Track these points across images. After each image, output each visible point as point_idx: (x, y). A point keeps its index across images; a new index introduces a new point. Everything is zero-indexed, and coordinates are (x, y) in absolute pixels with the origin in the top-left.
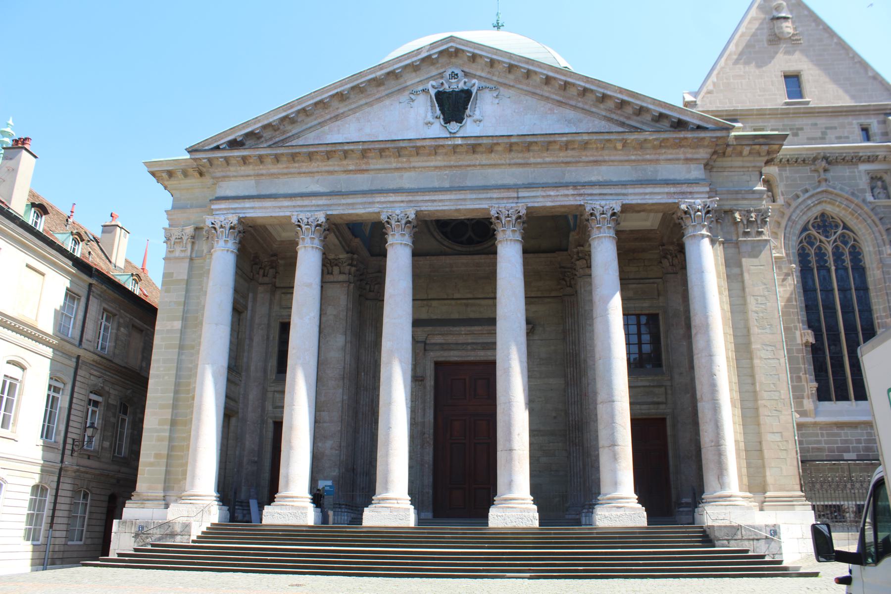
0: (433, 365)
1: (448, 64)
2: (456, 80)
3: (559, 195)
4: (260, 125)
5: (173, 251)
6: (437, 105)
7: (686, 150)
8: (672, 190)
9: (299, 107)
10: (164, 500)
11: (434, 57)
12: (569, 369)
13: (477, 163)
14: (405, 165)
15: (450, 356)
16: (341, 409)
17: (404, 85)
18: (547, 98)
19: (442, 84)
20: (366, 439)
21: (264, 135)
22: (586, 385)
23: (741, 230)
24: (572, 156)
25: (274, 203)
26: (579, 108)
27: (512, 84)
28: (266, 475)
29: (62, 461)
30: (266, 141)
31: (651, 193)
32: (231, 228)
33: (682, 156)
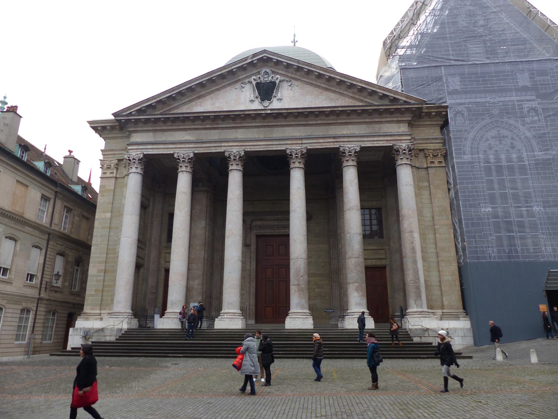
0: (255, 237)
1: (263, 66)
2: (267, 76)
3: (324, 142)
4: (155, 101)
5: (105, 173)
6: (256, 90)
7: (397, 115)
8: (389, 138)
9: (178, 91)
10: (100, 316)
11: (254, 62)
12: (331, 240)
13: (279, 124)
14: (239, 125)
16: (203, 262)
17: (238, 79)
18: (319, 87)
19: (260, 78)
21: (158, 107)
22: (341, 248)
23: (429, 162)
24: (333, 120)
25: (164, 146)
26: (337, 92)
27: (299, 78)
28: (160, 300)
29: (39, 294)
30: (159, 110)
31: (377, 141)
32: (139, 160)
33: (395, 119)
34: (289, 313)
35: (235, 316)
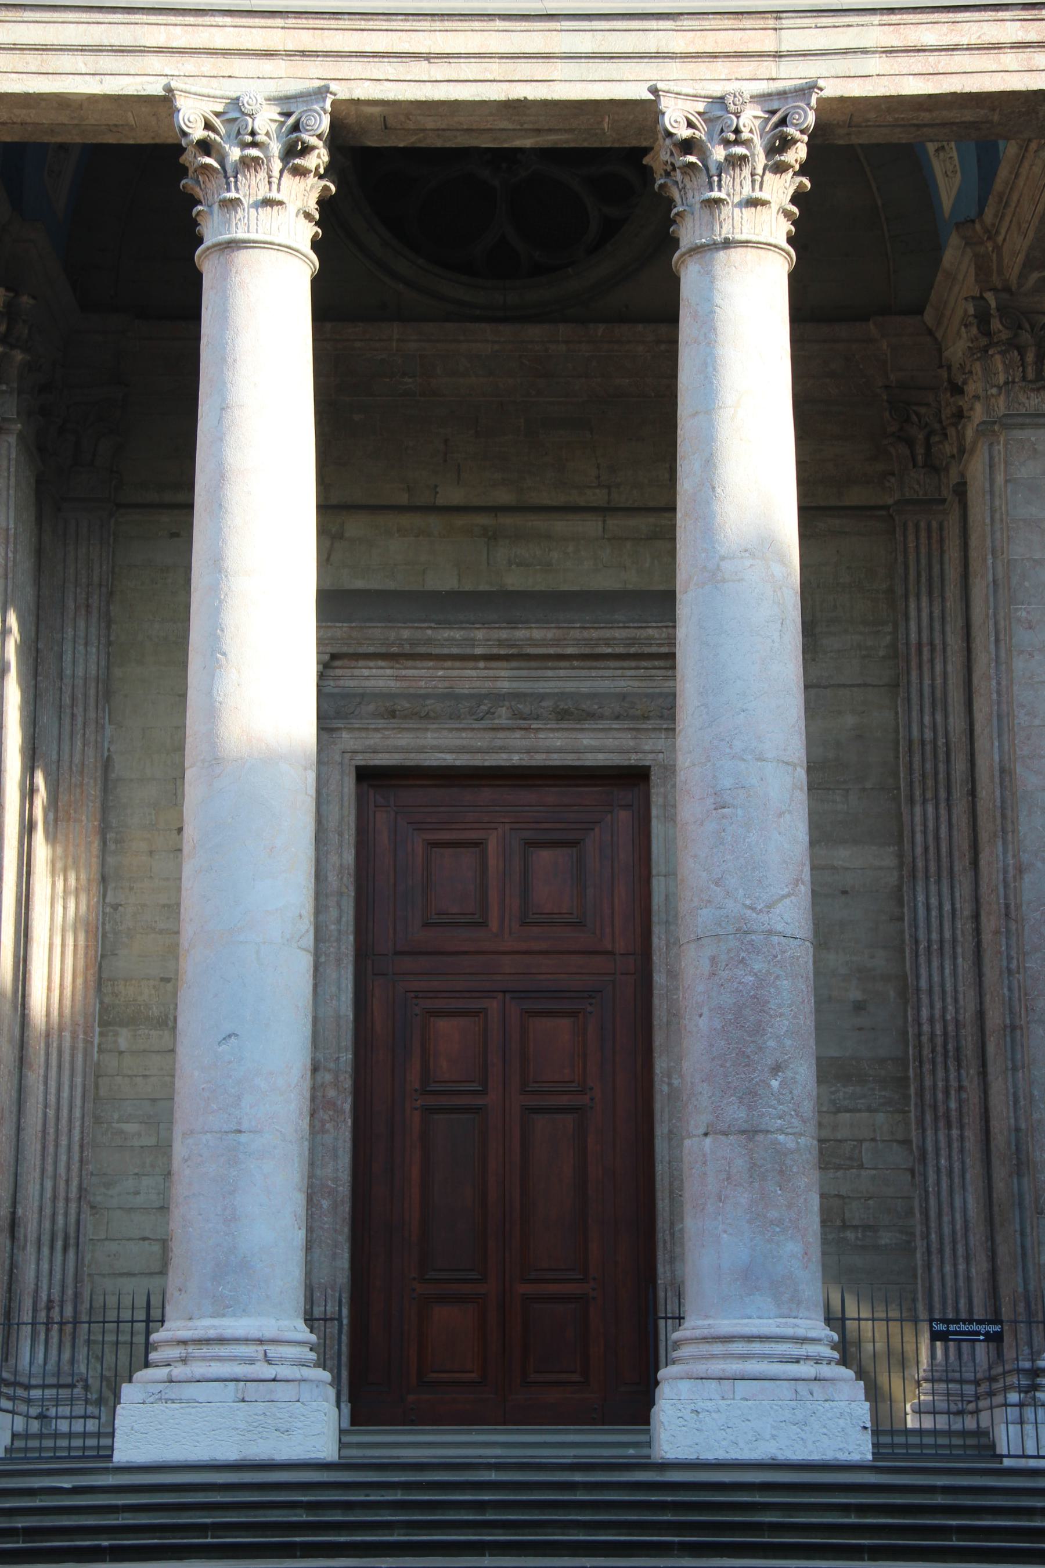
0: (349, 784)
12: (918, 810)
15: (421, 750)
20: (65, 1094)
34: (677, 1345)
35: (269, 1361)
